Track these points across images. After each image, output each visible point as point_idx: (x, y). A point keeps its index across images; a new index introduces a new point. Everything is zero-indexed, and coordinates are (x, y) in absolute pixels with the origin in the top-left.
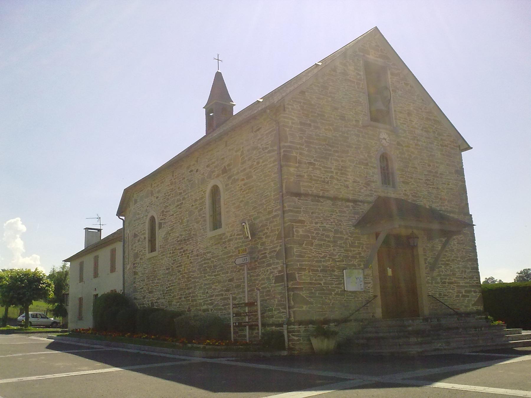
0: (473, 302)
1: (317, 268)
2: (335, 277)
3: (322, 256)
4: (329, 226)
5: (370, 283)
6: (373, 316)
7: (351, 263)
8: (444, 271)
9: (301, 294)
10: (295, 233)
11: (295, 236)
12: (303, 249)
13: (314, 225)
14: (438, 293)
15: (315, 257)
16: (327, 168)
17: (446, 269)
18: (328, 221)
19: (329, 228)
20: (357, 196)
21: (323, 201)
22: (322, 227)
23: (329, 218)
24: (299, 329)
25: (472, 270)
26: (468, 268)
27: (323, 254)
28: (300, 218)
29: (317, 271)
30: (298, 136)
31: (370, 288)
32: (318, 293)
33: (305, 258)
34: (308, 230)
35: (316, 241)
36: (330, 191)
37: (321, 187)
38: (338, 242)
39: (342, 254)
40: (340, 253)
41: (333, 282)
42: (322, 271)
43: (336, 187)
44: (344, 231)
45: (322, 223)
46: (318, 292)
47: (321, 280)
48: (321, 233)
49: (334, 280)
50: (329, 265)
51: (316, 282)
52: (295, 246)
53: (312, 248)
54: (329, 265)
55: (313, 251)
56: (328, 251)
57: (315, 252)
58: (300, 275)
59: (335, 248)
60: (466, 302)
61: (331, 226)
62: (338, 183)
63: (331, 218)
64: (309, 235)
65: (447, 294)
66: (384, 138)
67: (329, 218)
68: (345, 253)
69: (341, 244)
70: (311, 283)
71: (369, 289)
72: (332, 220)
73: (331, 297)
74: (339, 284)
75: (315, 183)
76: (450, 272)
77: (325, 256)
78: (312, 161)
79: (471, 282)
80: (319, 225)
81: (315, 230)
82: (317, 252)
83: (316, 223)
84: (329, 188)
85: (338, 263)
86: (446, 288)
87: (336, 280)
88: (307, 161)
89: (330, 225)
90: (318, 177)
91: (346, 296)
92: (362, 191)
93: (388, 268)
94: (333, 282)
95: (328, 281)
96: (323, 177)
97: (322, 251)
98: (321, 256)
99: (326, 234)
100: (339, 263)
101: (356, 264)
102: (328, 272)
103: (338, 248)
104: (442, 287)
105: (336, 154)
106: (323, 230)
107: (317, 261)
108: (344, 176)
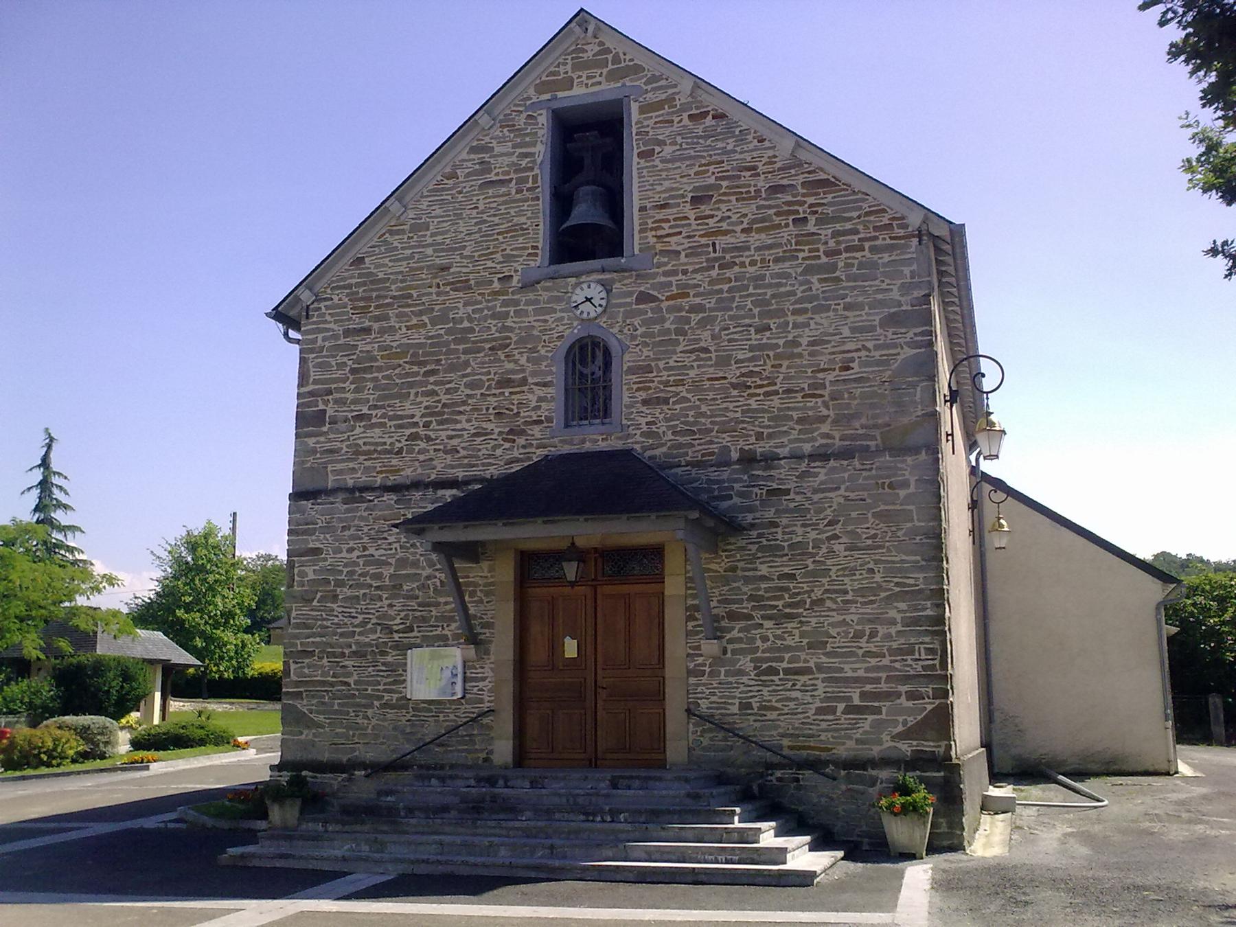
0: (900, 728)
1: (343, 648)
2: (384, 668)
3: (358, 622)
4: (383, 552)
5: (484, 679)
6: (485, 760)
7: (434, 633)
8: (772, 638)
9: (299, 706)
10: (296, 578)
11: (295, 583)
12: (312, 610)
13: (344, 554)
14: (737, 701)
15: (338, 625)
16: (401, 417)
17: (779, 632)
18: (380, 542)
19: (382, 558)
20: (481, 468)
21: (371, 498)
22: (365, 556)
23: (385, 535)
24: (279, 778)
25: (904, 629)
26: (893, 622)
27: (361, 617)
28: (311, 546)
29: (343, 655)
30: (334, 363)
31: (484, 690)
32: (339, 704)
33: (314, 630)
34: (329, 567)
35: (345, 590)
36: (404, 469)
37: (380, 464)
38: (405, 587)
39: (410, 613)
40: (405, 613)
41: (379, 679)
42: (355, 654)
43: (422, 457)
44: (422, 558)
45: (365, 549)
46: (339, 701)
47: (349, 675)
48: (360, 572)
49: (382, 674)
50: (374, 640)
51: (334, 680)
52: (294, 605)
53: (334, 606)
54: (374, 640)
55: (336, 613)
56: (374, 608)
57: (340, 615)
58: (299, 665)
59: (395, 602)
60: (867, 728)
61: (389, 552)
62: (428, 448)
63: (390, 535)
64: (331, 578)
65: (779, 705)
66: (586, 298)
67: (385, 535)
68: (421, 611)
69: (412, 589)
70: (323, 683)
71: (483, 695)
72: (392, 539)
73: (370, 712)
74: (395, 682)
75: (365, 460)
76: (797, 639)
77: (367, 622)
78: (365, 410)
79: (897, 665)
80: (356, 553)
81: (346, 565)
82: (346, 615)
83: (350, 550)
84: (401, 463)
85: (396, 636)
86: (774, 687)
87: (385, 674)
88: (350, 415)
89: (385, 549)
90: (376, 444)
91: (411, 710)
92: (499, 452)
93: (568, 640)
94: (379, 679)
95: (367, 677)
96: (389, 441)
97: (359, 610)
98: (357, 622)
99: (371, 572)
100: (401, 635)
101: (449, 633)
102: (369, 657)
103: (402, 600)
104: (760, 683)
105: (432, 379)
106: (365, 564)
107: (342, 635)
108: (445, 427)
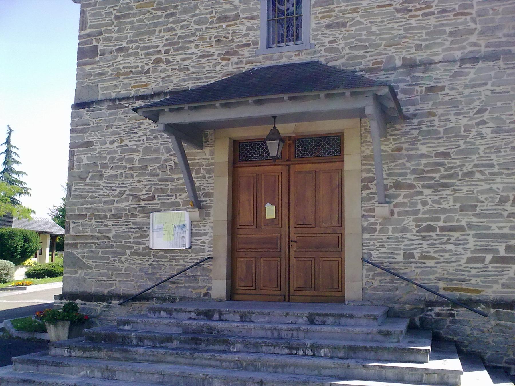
1: (105, 212)
2: (134, 227)
4: (134, 143)
5: (205, 234)
6: (206, 294)
7: (170, 201)
8: (430, 203)
10: (76, 163)
11: (75, 167)
13: (108, 145)
14: (402, 252)
16: (149, 48)
17: (436, 198)
18: (132, 135)
20: (205, 80)
21: (127, 105)
22: (122, 146)
23: (136, 130)
27: (118, 190)
28: (86, 140)
29: (106, 217)
30: (103, 13)
32: (102, 252)
33: (87, 200)
34: (98, 155)
35: (108, 170)
37: (134, 81)
38: (149, 168)
39: (153, 186)
43: (163, 75)
44: (162, 146)
45: (122, 141)
47: (110, 231)
48: (118, 157)
49: (132, 230)
51: (99, 235)
53: (101, 182)
55: (101, 187)
56: (127, 183)
58: (76, 224)
59: (142, 178)
61: (139, 143)
62: (167, 68)
63: (140, 130)
64: (99, 162)
65: (436, 255)
67: (136, 130)
68: (161, 185)
69: (154, 169)
70: (92, 237)
71: (204, 246)
72: (140, 133)
73: (123, 258)
78: (125, 45)
80: (116, 144)
81: (109, 153)
82: (108, 188)
83: (112, 142)
84: (148, 80)
85: (143, 203)
88: (114, 48)
89: (136, 141)
90: (132, 67)
92: (218, 68)
96: (140, 65)
97: (117, 185)
98: (116, 193)
99: (127, 157)
100: (146, 202)
101: (180, 201)
102: (123, 218)
103: (147, 177)
104: (421, 238)
105: (171, 20)
107: (105, 203)
108: (180, 52)
